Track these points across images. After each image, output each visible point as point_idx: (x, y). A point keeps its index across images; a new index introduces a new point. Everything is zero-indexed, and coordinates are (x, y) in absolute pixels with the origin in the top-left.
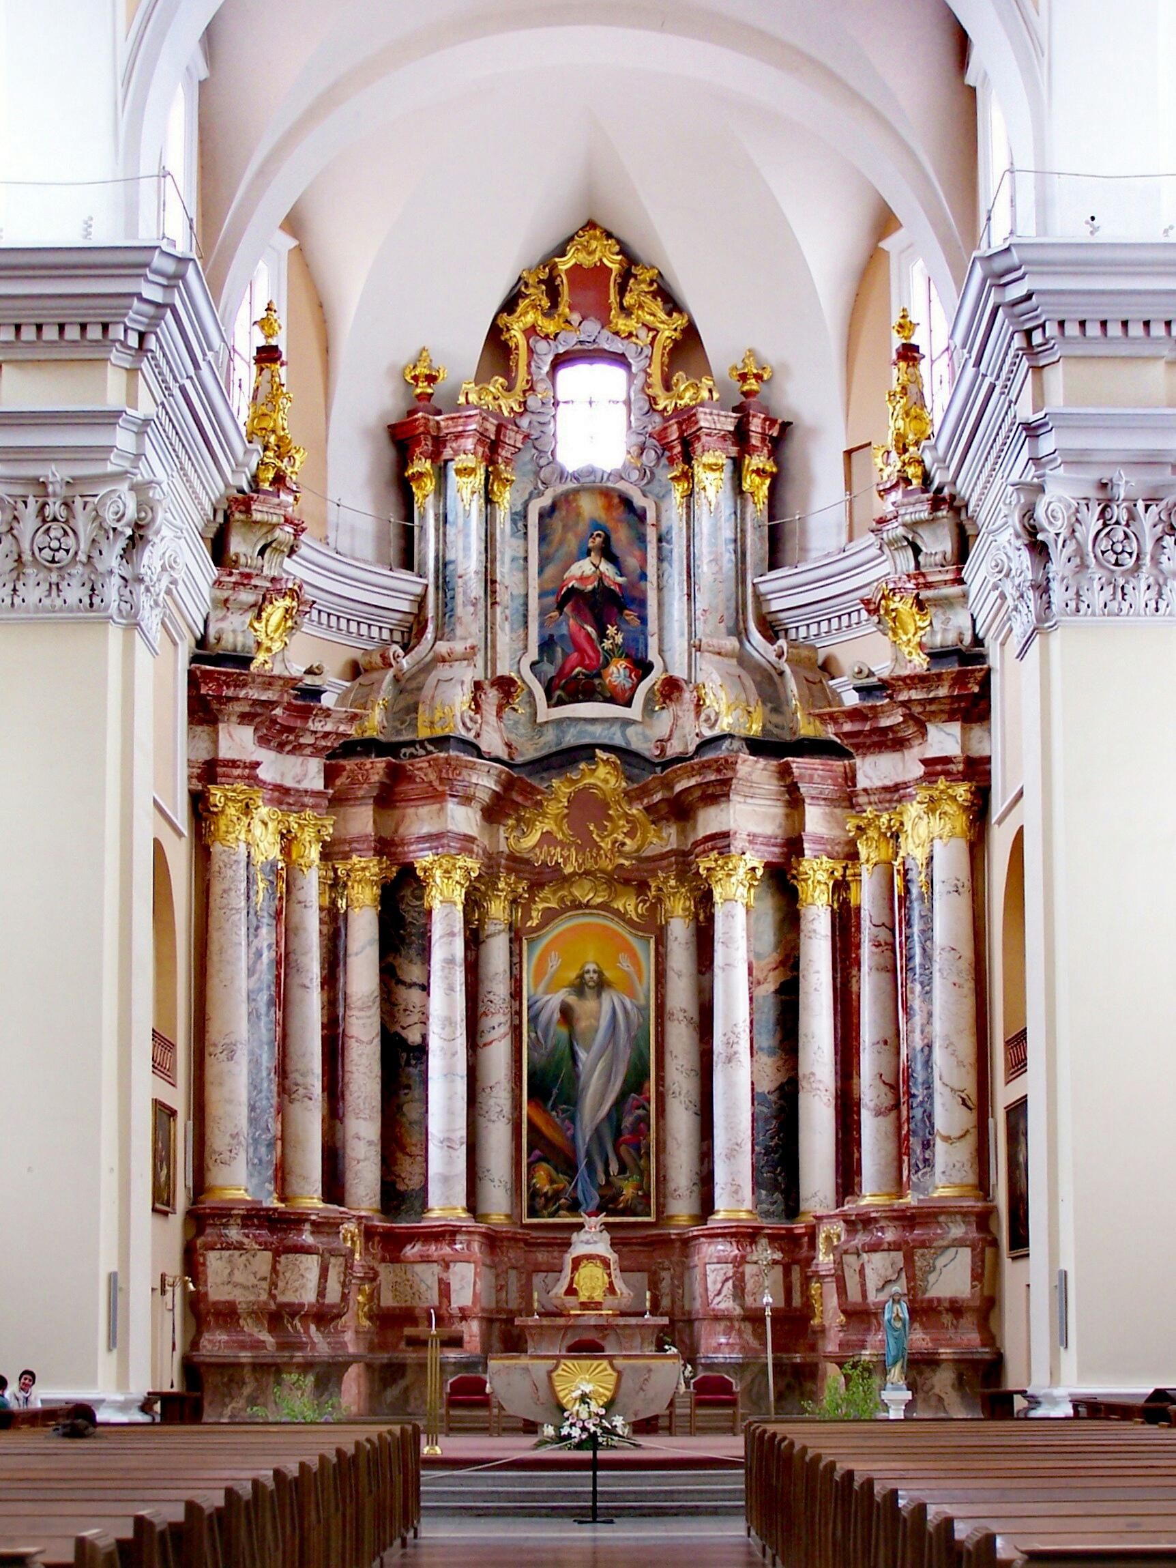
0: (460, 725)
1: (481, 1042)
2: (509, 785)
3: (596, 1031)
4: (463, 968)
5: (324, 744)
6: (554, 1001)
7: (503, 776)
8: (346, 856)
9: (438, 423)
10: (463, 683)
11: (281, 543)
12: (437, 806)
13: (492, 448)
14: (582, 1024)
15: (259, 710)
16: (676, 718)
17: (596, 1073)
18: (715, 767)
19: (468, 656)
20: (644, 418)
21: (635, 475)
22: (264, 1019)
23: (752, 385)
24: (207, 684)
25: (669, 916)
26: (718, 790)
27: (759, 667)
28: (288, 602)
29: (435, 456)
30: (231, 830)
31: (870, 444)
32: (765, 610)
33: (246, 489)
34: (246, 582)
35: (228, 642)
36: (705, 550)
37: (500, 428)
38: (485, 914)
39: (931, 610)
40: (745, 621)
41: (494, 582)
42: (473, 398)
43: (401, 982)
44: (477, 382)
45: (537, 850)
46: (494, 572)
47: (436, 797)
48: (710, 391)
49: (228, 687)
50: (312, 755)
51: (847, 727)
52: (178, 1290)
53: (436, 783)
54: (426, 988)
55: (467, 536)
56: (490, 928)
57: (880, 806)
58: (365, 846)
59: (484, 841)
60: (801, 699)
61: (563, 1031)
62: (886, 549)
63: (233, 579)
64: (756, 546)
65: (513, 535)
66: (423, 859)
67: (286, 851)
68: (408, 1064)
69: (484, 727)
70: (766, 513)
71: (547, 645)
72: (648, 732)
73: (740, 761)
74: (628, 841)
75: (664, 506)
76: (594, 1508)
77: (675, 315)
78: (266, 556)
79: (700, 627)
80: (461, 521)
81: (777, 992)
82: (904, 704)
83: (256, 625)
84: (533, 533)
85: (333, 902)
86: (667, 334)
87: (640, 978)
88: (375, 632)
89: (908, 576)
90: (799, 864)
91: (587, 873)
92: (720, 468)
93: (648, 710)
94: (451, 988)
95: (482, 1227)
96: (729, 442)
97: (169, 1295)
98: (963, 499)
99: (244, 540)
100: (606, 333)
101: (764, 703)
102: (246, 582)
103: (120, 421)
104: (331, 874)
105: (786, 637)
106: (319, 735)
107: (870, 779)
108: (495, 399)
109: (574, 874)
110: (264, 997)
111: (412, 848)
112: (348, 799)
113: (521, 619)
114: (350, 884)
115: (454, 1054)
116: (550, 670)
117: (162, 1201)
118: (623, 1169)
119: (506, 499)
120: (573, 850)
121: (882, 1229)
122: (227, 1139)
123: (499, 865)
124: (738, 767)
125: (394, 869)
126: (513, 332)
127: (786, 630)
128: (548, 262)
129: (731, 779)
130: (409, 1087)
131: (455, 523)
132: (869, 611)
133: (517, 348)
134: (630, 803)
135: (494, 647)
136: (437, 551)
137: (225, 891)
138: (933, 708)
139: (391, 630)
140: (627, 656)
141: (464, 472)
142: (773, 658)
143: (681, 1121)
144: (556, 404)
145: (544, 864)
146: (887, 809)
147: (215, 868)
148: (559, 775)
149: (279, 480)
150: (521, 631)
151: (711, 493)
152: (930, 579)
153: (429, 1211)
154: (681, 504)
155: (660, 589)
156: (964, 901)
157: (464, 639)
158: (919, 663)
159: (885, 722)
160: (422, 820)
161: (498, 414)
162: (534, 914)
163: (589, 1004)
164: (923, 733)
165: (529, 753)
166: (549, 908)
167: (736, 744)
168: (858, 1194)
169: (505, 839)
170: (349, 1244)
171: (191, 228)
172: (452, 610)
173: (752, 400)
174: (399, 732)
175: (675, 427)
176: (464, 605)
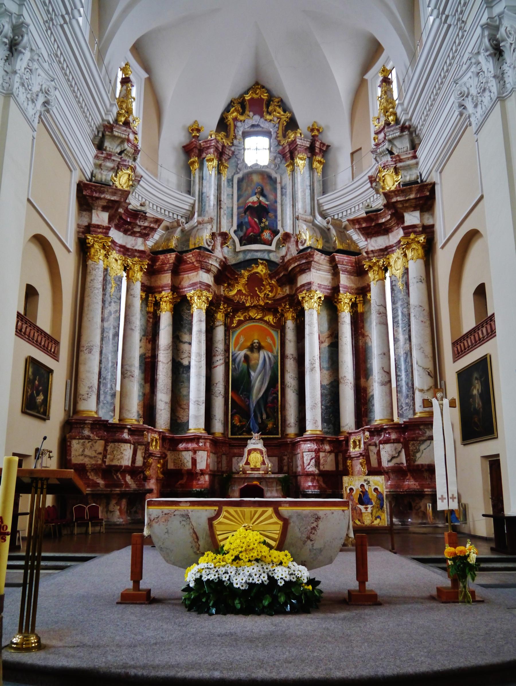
0: (205, 244)
4: (205, 334)
6: (242, 353)
7: (222, 263)
8: (160, 292)
9: (200, 144)
10: (207, 228)
11: (128, 152)
12: (196, 273)
13: (221, 154)
15: (110, 204)
18: (305, 257)
19: (211, 221)
20: (276, 148)
21: (273, 166)
23: (316, 133)
24: (86, 190)
25: (286, 319)
26: (306, 267)
28: (129, 172)
29: (199, 156)
30: (96, 254)
31: (360, 149)
32: (322, 209)
33: (112, 122)
34: (109, 157)
37: (223, 146)
39: (402, 172)
40: (314, 213)
41: (220, 201)
43: (182, 342)
44: (216, 131)
45: (236, 297)
46: (220, 197)
47: (194, 269)
48: (301, 134)
49: (96, 193)
50: (140, 237)
51: (364, 225)
53: (195, 263)
55: (210, 182)
56: (217, 323)
57: (379, 257)
58: (167, 288)
59: (214, 288)
61: (245, 365)
63: (103, 156)
64: (318, 187)
65: (228, 186)
66: (190, 293)
67: (127, 276)
68: (183, 373)
70: (321, 177)
71: (240, 226)
72: (278, 255)
73: (315, 254)
75: (283, 177)
80: (208, 178)
81: (329, 346)
83: (115, 179)
86: (285, 119)
87: (275, 346)
88: (175, 216)
90: (338, 295)
91: (255, 307)
92: (305, 159)
93: (278, 247)
94: (200, 342)
96: (308, 152)
98: (414, 127)
100: (262, 120)
101: (323, 239)
102: (109, 157)
104: (154, 299)
106: (142, 228)
107: (374, 247)
108: (222, 139)
109: (249, 307)
111: (186, 289)
112: (162, 271)
113: (231, 215)
114: (161, 303)
116: (241, 234)
118: (268, 417)
119: (226, 175)
122: (87, 389)
123: (221, 300)
124: (314, 256)
126: (229, 119)
128: (242, 96)
129: (312, 261)
130: (183, 382)
131: (206, 179)
133: (230, 124)
134: (271, 279)
135: (220, 223)
137: (92, 280)
138: (407, 205)
140: (270, 229)
142: (325, 224)
143: (291, 397)
144: (244, 149)
145: (238, 302)
147: (88, 271)
150: (230, 220)
151: (301, 167)
152: (402, 157)
153: (189, 430)
154: (290, 175)
155: (282, 205)
162: (235, 322)
169: (223, 291)
172: (205, 209)
175: (288, 147)
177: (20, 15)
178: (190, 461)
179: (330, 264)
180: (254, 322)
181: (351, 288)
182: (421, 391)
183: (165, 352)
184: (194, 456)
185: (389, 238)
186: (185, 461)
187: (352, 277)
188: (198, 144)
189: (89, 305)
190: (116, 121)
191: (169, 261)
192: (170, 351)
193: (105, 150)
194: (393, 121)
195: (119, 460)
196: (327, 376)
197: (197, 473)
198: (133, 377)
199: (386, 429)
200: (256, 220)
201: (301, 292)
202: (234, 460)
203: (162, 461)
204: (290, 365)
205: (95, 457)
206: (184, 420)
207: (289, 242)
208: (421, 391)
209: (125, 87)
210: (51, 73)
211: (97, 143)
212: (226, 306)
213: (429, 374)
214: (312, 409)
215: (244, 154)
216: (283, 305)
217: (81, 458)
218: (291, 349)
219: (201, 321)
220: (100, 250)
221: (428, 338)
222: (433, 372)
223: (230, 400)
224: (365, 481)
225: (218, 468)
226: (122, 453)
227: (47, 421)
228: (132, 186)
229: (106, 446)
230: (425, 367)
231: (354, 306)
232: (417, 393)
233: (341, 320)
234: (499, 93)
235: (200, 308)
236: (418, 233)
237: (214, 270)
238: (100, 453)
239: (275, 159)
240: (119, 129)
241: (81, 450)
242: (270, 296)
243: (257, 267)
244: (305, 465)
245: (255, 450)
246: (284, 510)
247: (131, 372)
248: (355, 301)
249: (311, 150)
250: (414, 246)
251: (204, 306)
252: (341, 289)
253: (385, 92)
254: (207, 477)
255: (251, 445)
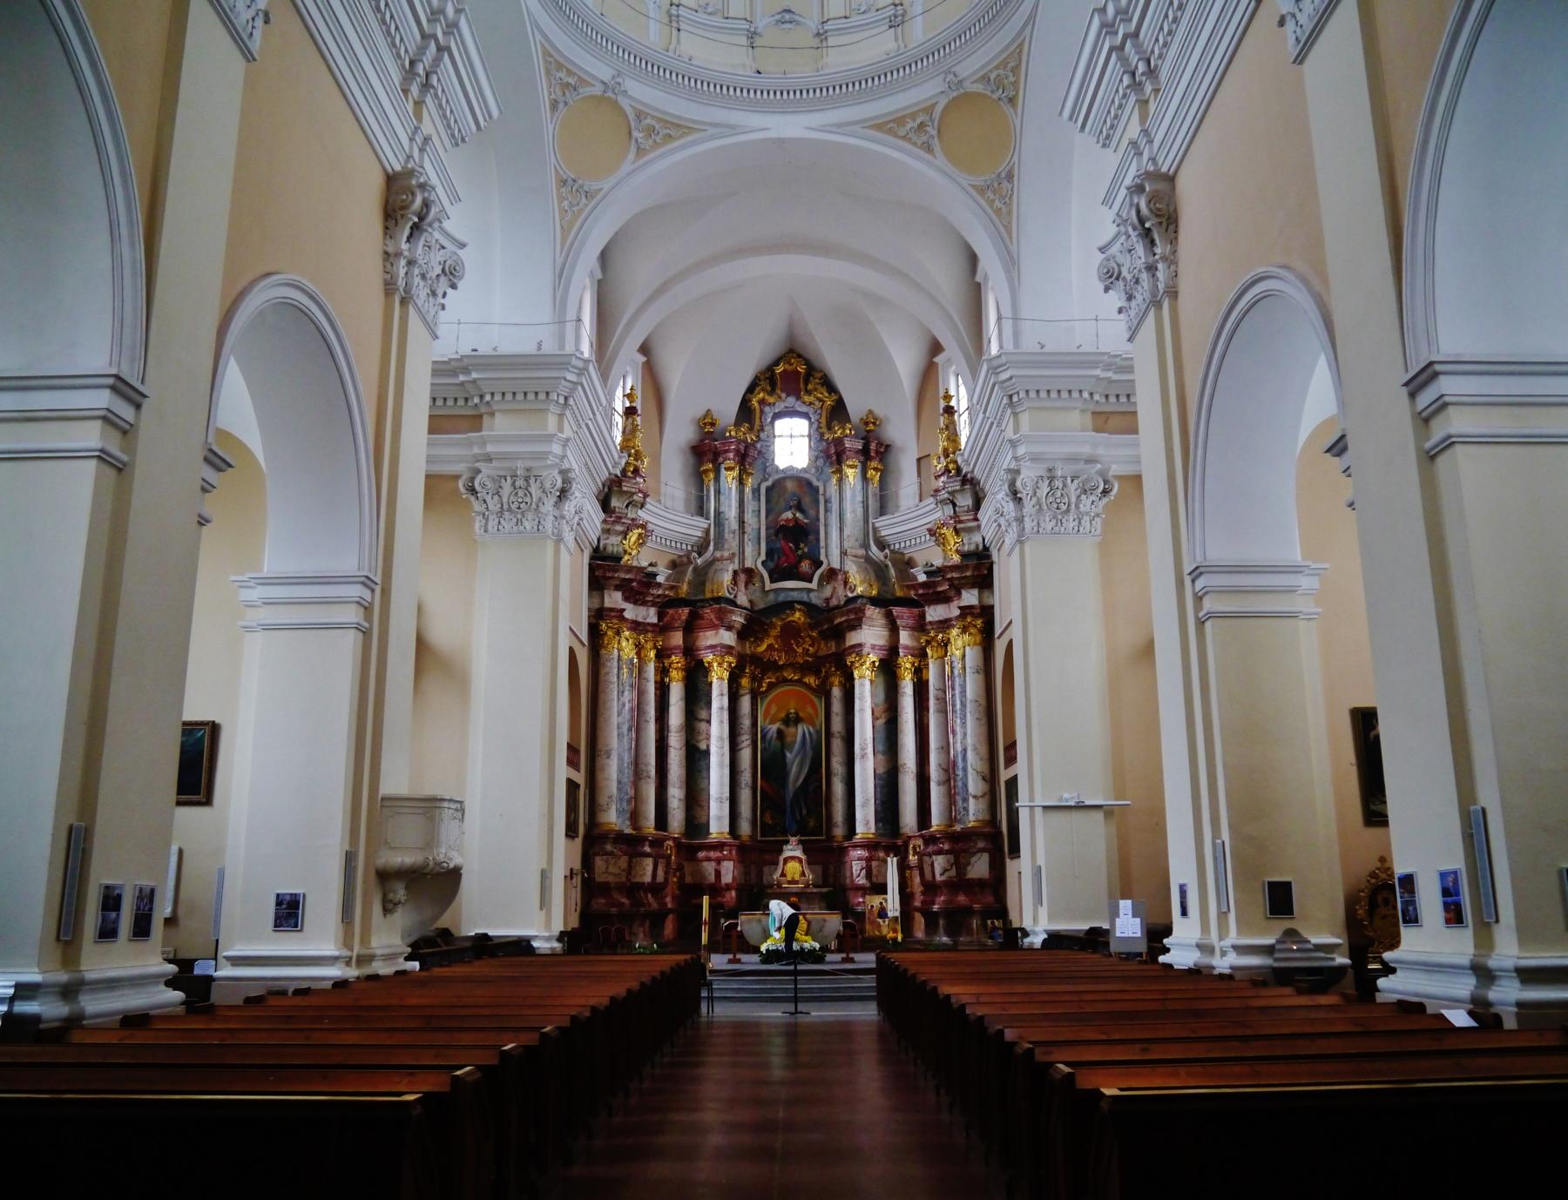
0: (726, 592)
1: (740, 747)
2: (749, 619)
3: (795, 742)
5: (658, 600)
6: (774, 728)
8: (670, 657)
10: (728, 571)
11: (637, 502)
14: (789, 739)
16: (835, 588)
17: (796, 763)
19: (731, 558)
21: (813, 471)
22: (626, 738)
23: (871, 427)
27: (876, 562)
28: (640, 530)
32: (878, 535)
33: (619, 474)
35: (610, 549)
36: (848, 506)
38: (739, 685)
39: (962, 534)
40: (869, 540)
41: (743, 522)
42: (733, 433)
47: (715, 627)
48: (850, 431)
51: (921, 592)
52: (579, 877)
53: (714, 620)
54: (709, 722)
55: (730, 500)
56: (742, 692)
58: (679, 651)
59: (739, 649)
60: (897, 579)
61: (778, 744)
62: (939, 505)
63: (612, 519)
64: (873, 505)
66: (709, 657)
67: (638, 654)
68: (700, 760)
69: (739, 593)
70: (878, 488)
71: (770, 553)
74: (811, 648)
76: (796, 997)
77: (833, 394)
78: (629, 508)
79: (846, 544)
80: (727, 492)
82: (949, 580)
84: (763, 499)
85: (662, 679)
86: (829, 403)
89: (951, 517)
92: (855, 467)
93: (820, 584)
94: (722, 722)
95: (737, 842)
97: (574, 880)
99: (618, 500)
100: (799, 402)
101: (878, 581)
103: (555, 440)
105: (889, 548)
110: (625, 728)
113: (756, 540)
115: (723, 755)
116: (771, 565)
117: (571, 831)
120: (783, 654)
121: (942, 843)
125: (693, 663)
127: (889, 545)
130: (700, 771)
131: (724, 494)
132: (931, 535)
134: (812, 630)
136: (715, 507)
139: (692, 546)
140: (810, 559)
141: (728, 469)
142: (882, 558)
144: (774, 437)
146: (941, 632)
148: (775, 617)
149: (636, 471)
150: (757, 546)
151: (851, 478)
152: (962, 518)
155: (826, 525)
156: (981, 677)
157: (729, 550)
158: (956, 559)
159: (940, 589)
160: (707, 638)
161: (745, 441)
162: (764, 685)
163: (792, 730)
164: (959, 594)
165: (761, 605)
166: (772, 682)
167: (865, 601)
168: (931, 827)
170: (669, 852)
171: (592, 346)
172: (723, 536)
173: (871, 434)
174: (696, 595)
176: (729, 533)
177: (564, 457)
178: (713, 873)
179: (886, 618)
180: (789, 685)
181: (913, 648)
182: (975, 797)
183: (677, 735)
184: (718, 868)
185: (949, 608)
186: (707, 874)
187: (916, 633)
188: (713, 446)
189: (604, 703)
190: (624, 471)
191: (679, 619)
192: (683, 733)
193: (614, 512)
194: (953, 469)
195: (641, 876)
196: (883, 763)
197: (722, 888)
198: (649, 777)
199: (939, 838)
200: (791, 545)
201: (850, 654)
202: (766, 869)
203: (678, 874)
204: (837, 745)
205: (619, 874)
206: (703, 820)
207: (836, 580)
208: (975, 797)
209: (630, 420)
210: (584, 490)
211: (601, 498)
212: (753, 668)
213: (984, 778)
214: (863, 806)
215: (774, 452)
216: (827, 665)
217: (605, 875)
218: (837, 724)
219: (722, 695)
220: (614, 637)
221: (983, 738)
222: (988, 776)
223: (759, 788)
224: (884, 899)
225: (745, 880)
226: (644, 869)
227: (576, 839)
228: (641, 544)
229: (630, 862)
230: (979, 770)
231: (919, 672)
232: (971, 801)
233: (901, 691)
234: (1018, 537)
235: (721, 679)
236: (975, 616)
237: (738, 626)
238: (624, 870)
239: (816, 461)
240: (628, 482)
241: (605, 867)
242: (810, 652)
243: (793, 614)
244: (855, 876)
245: (793, 858)
246: (808, 917)
247: (647, 772)
248: (919, 665)
249: (865, 454)
250: (973, 630)
251: (726, 675)
252: (900, 650)
253: (947, 428)
254: (733, 893)
255: (787, 854)
